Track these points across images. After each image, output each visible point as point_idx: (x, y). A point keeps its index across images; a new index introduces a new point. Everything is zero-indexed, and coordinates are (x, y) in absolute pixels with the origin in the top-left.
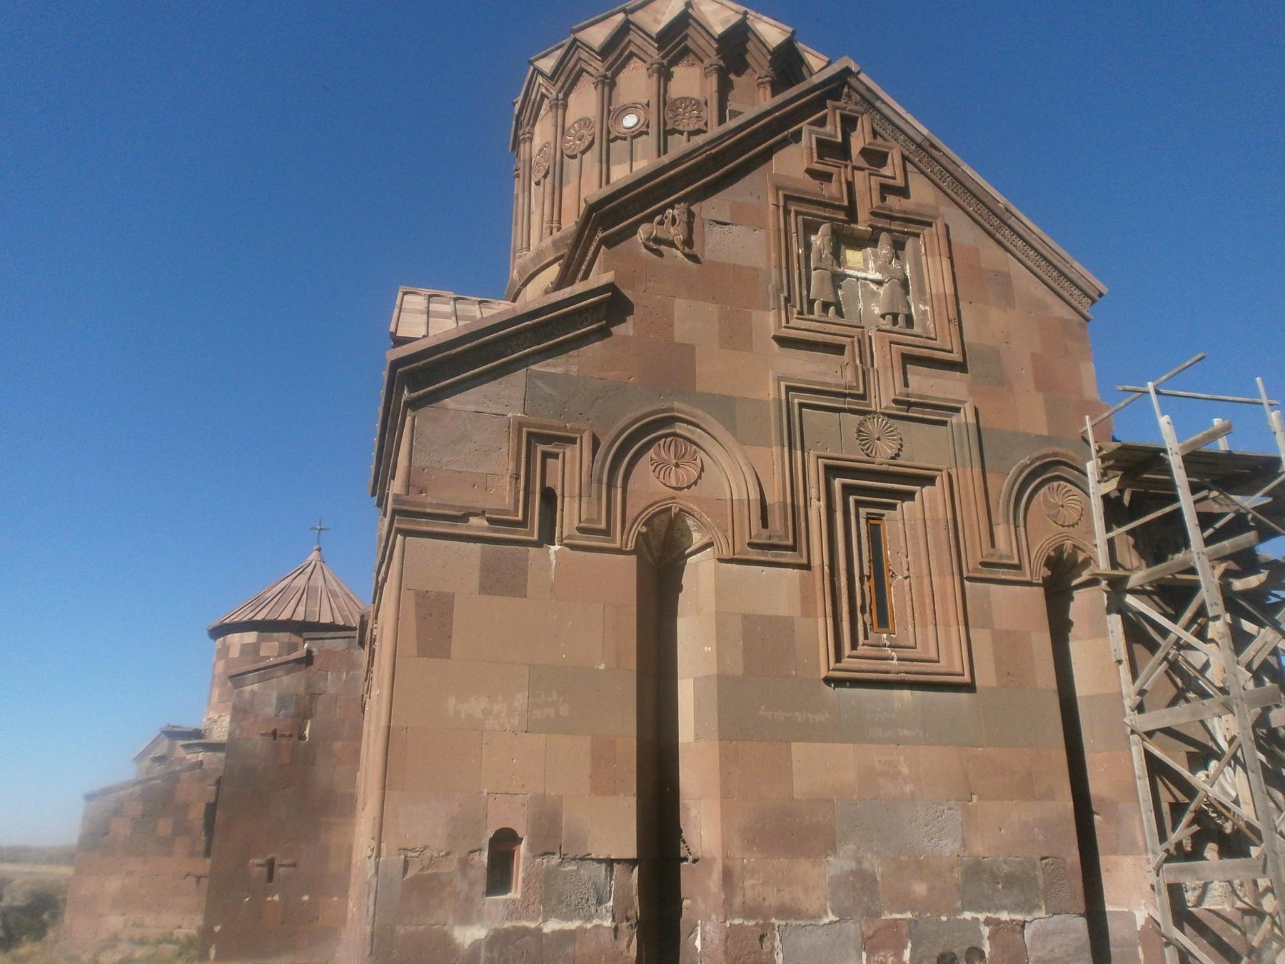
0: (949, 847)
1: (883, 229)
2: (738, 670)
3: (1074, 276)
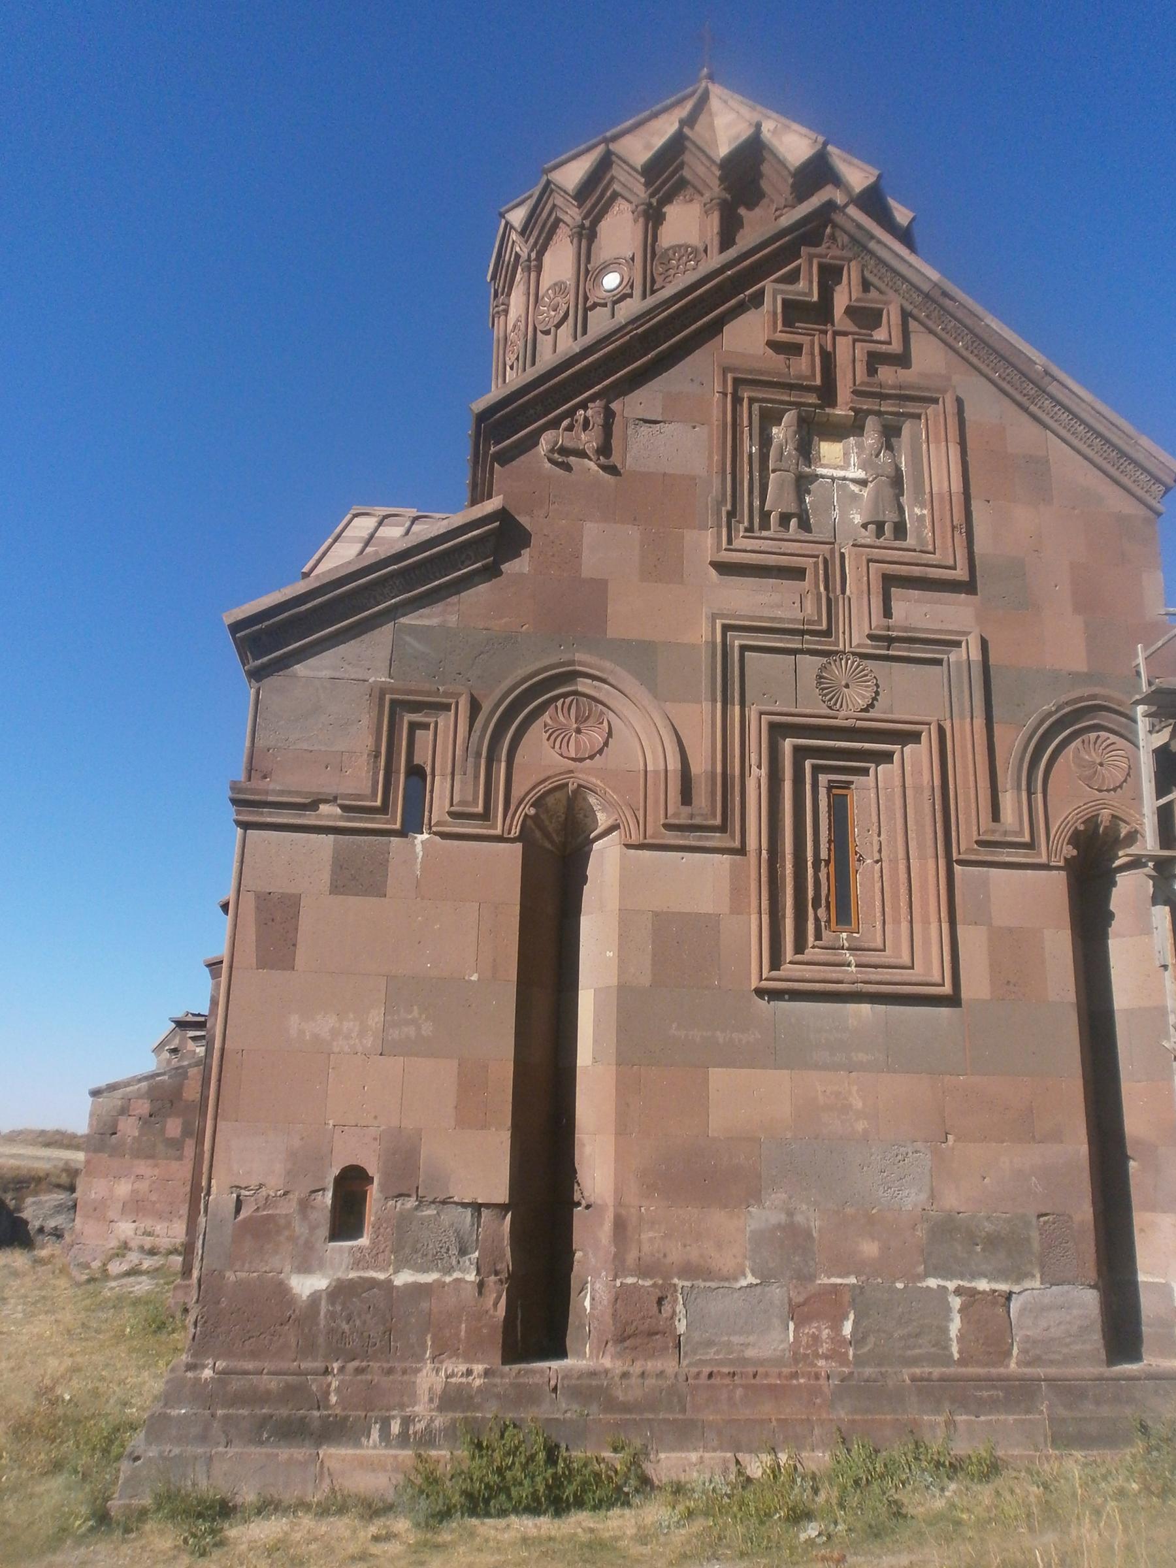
0: (912, 1198)
1: (869, 412)
2: (645, 980)
3: (1140, 457)
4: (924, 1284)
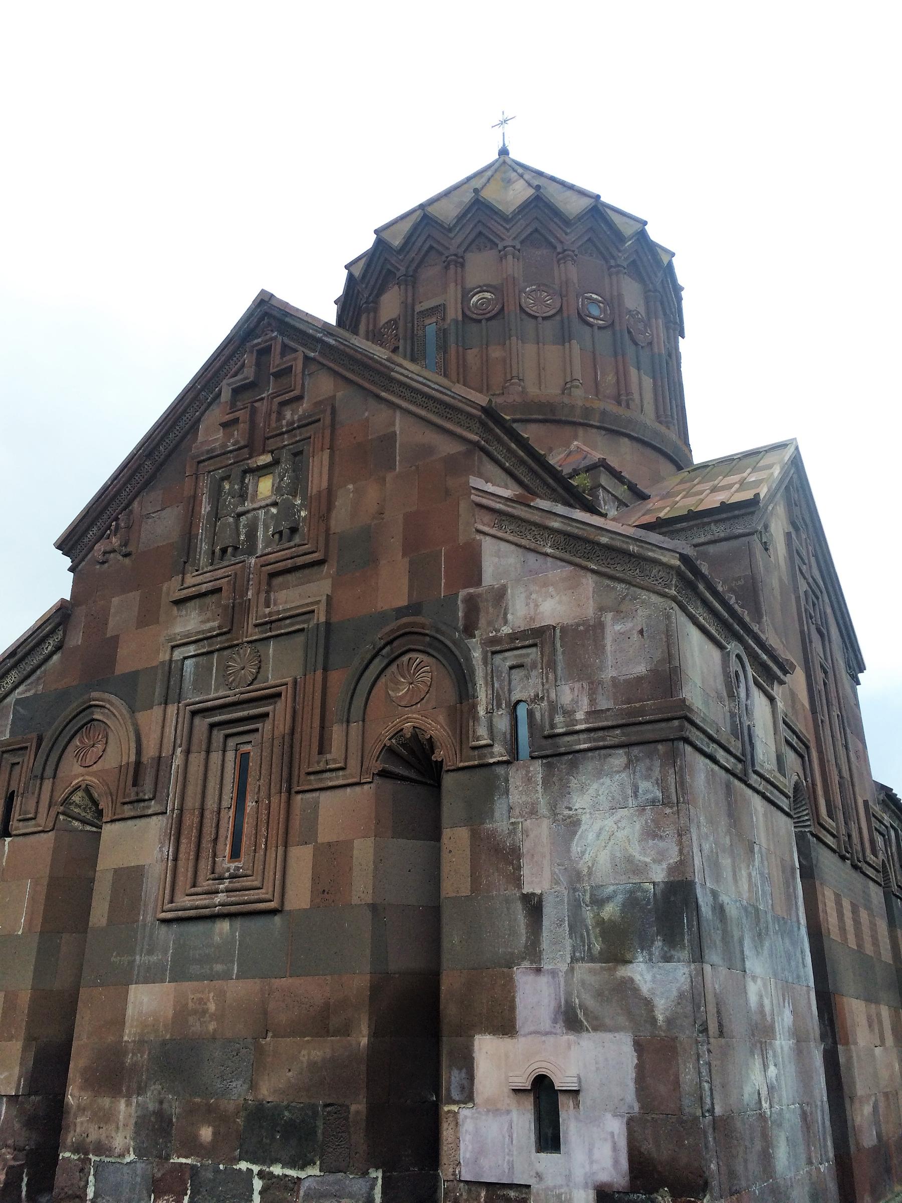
0: (238, 1090)
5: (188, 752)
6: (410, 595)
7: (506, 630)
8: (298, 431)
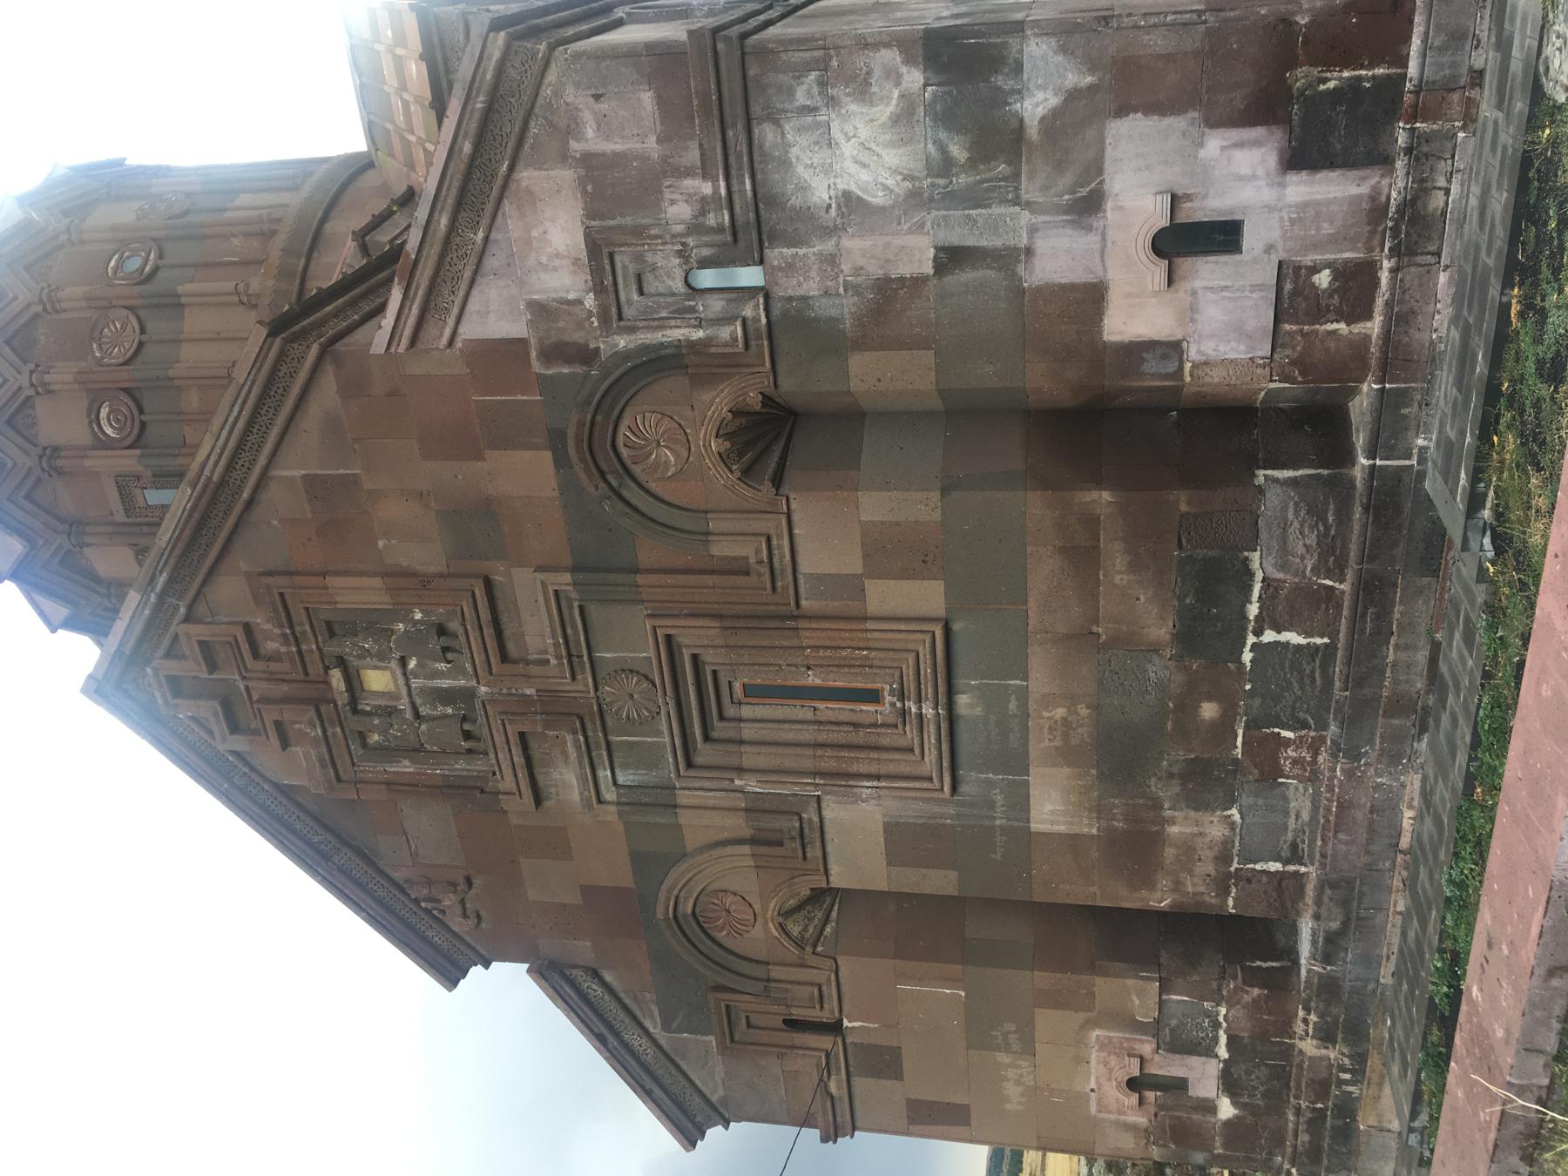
0: (1158, 670)
4: (1248, 664)
5: (740, 770)
6: (536, 447)
7: (590, 301)
8: (298, 629)
